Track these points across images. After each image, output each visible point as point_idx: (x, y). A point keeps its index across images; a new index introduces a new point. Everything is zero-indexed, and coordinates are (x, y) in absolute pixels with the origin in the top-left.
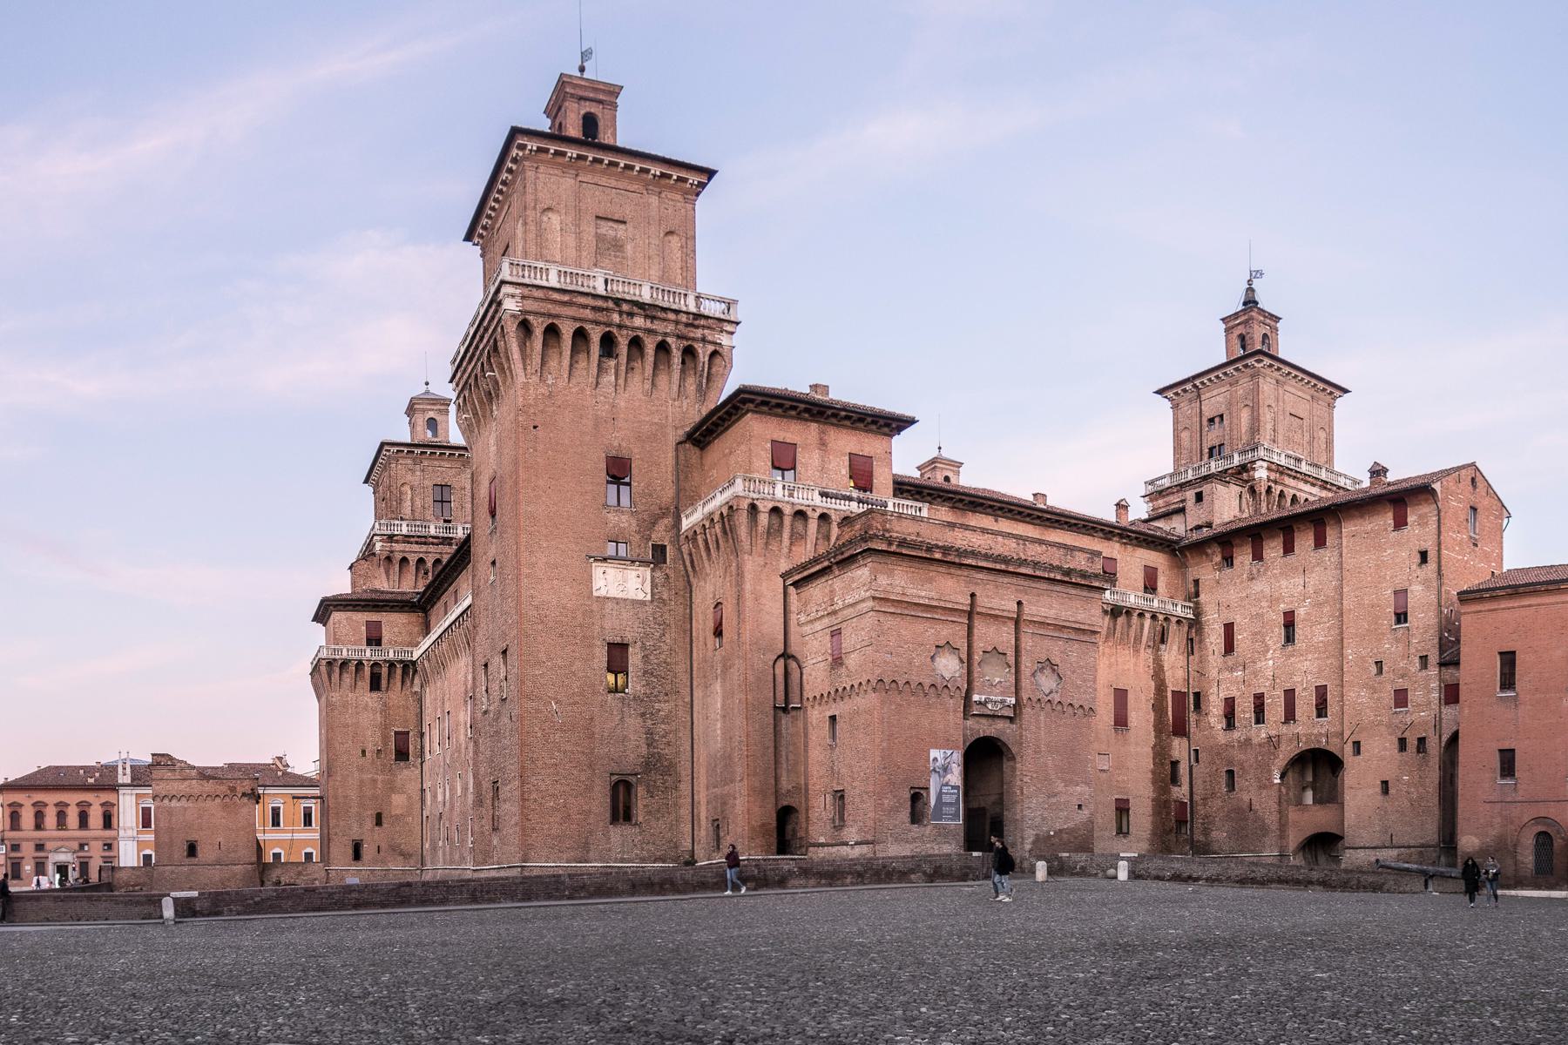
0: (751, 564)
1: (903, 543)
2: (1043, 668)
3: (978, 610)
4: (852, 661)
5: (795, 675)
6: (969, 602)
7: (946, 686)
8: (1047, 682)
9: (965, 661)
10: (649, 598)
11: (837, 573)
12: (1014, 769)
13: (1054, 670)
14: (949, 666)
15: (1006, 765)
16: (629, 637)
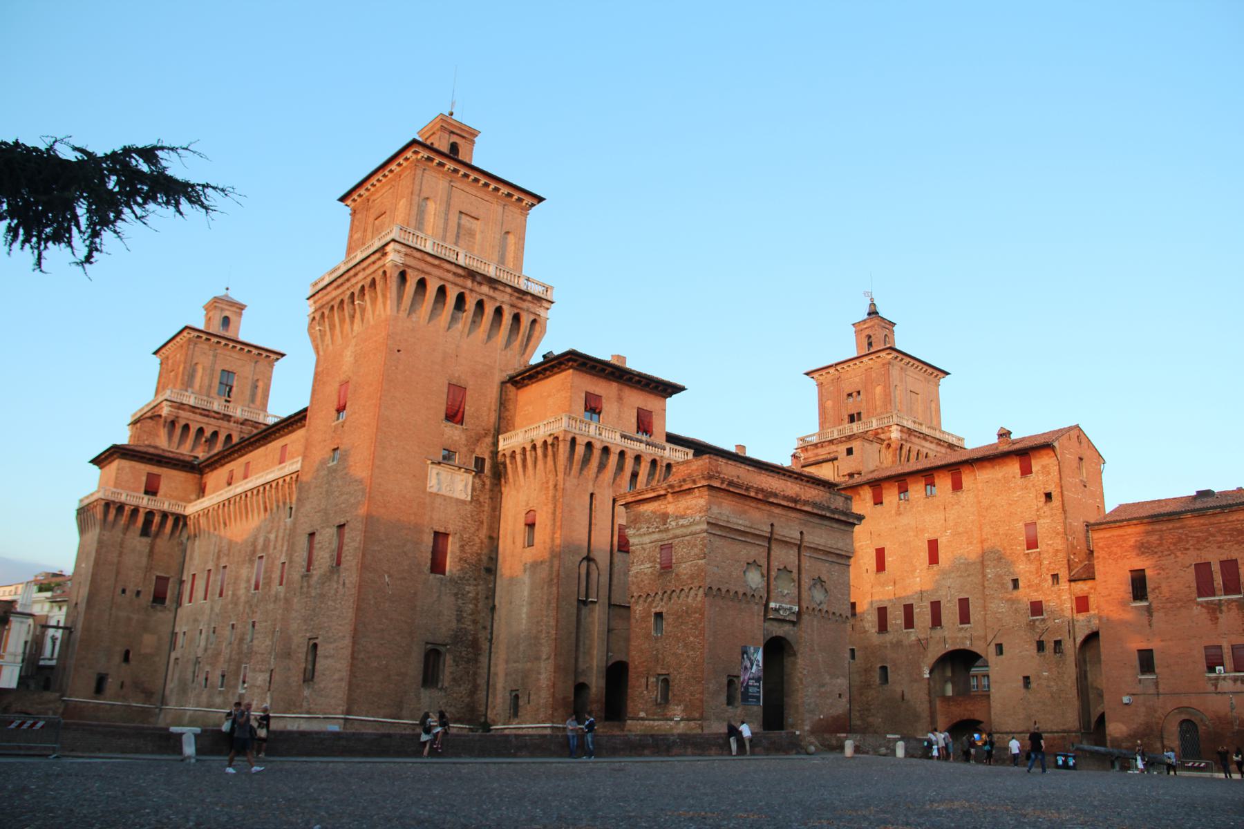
1: (731, 483)
2: (814, 585)
3: (776, 537)
5: (594, 575)
6: (769, 530)
7: (753, 595)
8: (818, 595)
9: (766, 575)
10: (469, 498)
12: (794, 663)
13: (822, 586)
14: (754, 579)
15: (788, 661)
16: (451, 529)
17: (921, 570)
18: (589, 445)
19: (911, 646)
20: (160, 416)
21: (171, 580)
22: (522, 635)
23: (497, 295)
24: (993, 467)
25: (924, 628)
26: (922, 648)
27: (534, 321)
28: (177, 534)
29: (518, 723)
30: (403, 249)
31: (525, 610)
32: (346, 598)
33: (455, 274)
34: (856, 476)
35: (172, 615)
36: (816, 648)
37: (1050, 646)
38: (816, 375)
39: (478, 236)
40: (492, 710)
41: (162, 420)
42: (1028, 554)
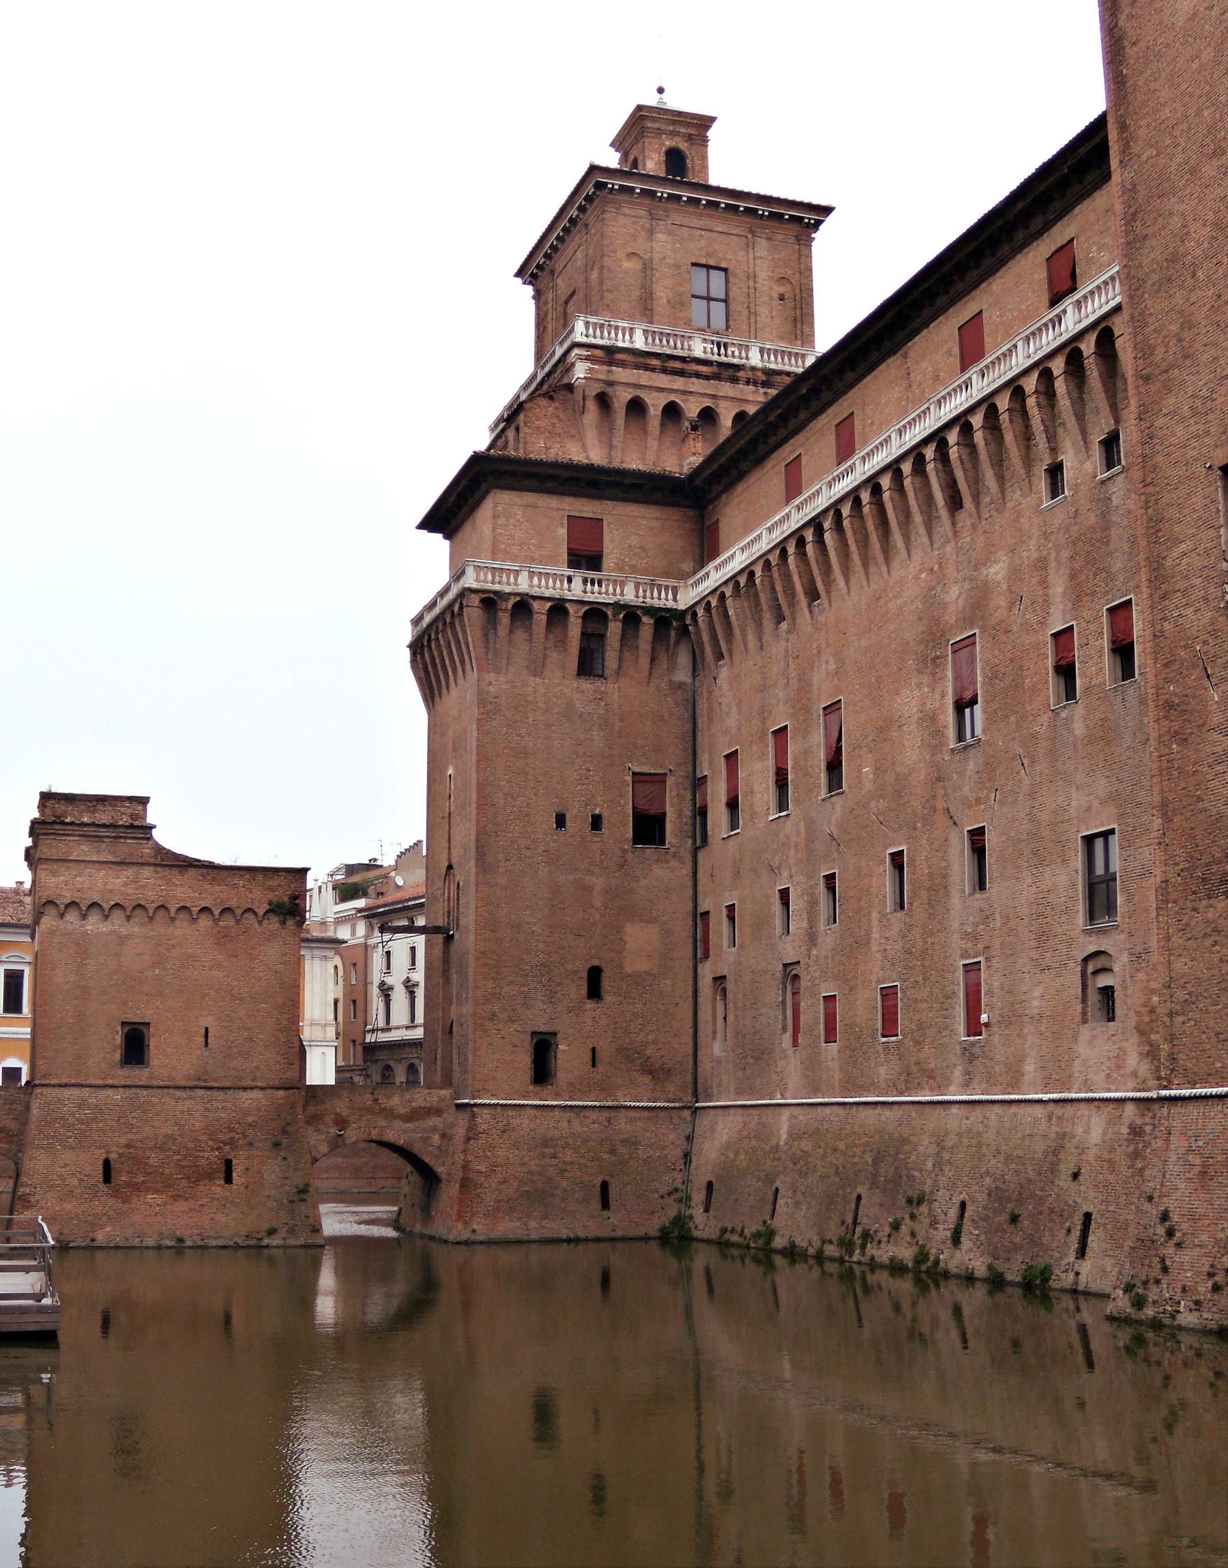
20: (570, 388)
21: (670, 781)
35: (686, 870)
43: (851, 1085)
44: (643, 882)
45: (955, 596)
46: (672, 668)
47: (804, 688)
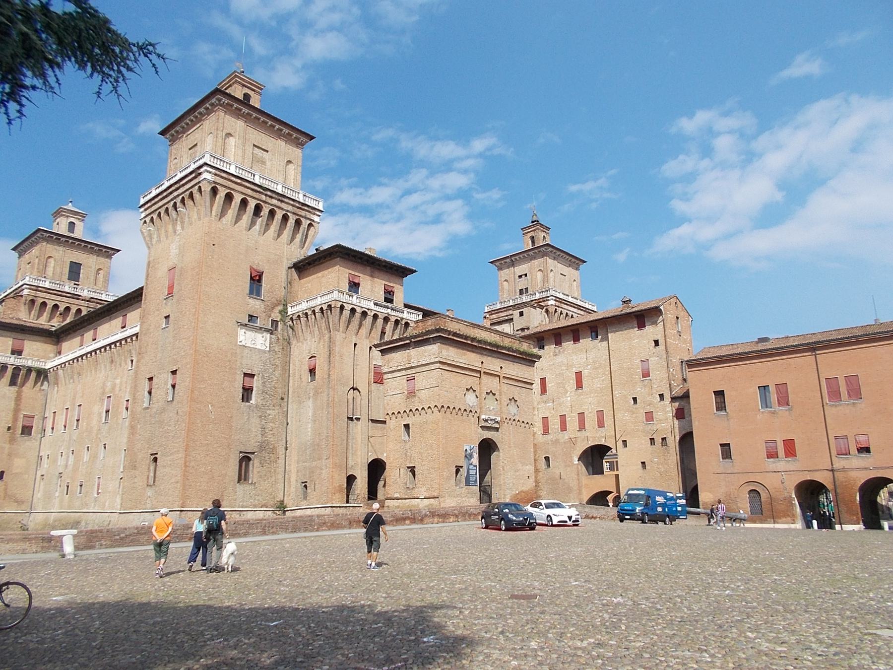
0: (339, 336)
4: (423, 394)
8: (513, 409)
10: (268, 349)
11: (414, 346)
17: (571, 392)
18: (353, 311)
19: (565, 443)
21: (36, 417)
22: (308, 443)
23: (283, 205)
24: (619, 324)
25: (573, 430)
26: (572, 444)
27: (310, 225)
28: (39, 384)
29: (308, 505)
30: (213, 171)
31: (310, 426)
32: (179, 423)
33: (252, 190)
34: (526, 330)
35: (38, 443)
36: (512, 445)
37: (658, 441)
38: (498, 264)
39: (268, 163)
40: (288, 497)
41: (24, 298)
42: (643, 380)
43: (69, 507)
44: (22, 447)
45: (109, 384)
46: (42, 385)
47: (74, 399)
